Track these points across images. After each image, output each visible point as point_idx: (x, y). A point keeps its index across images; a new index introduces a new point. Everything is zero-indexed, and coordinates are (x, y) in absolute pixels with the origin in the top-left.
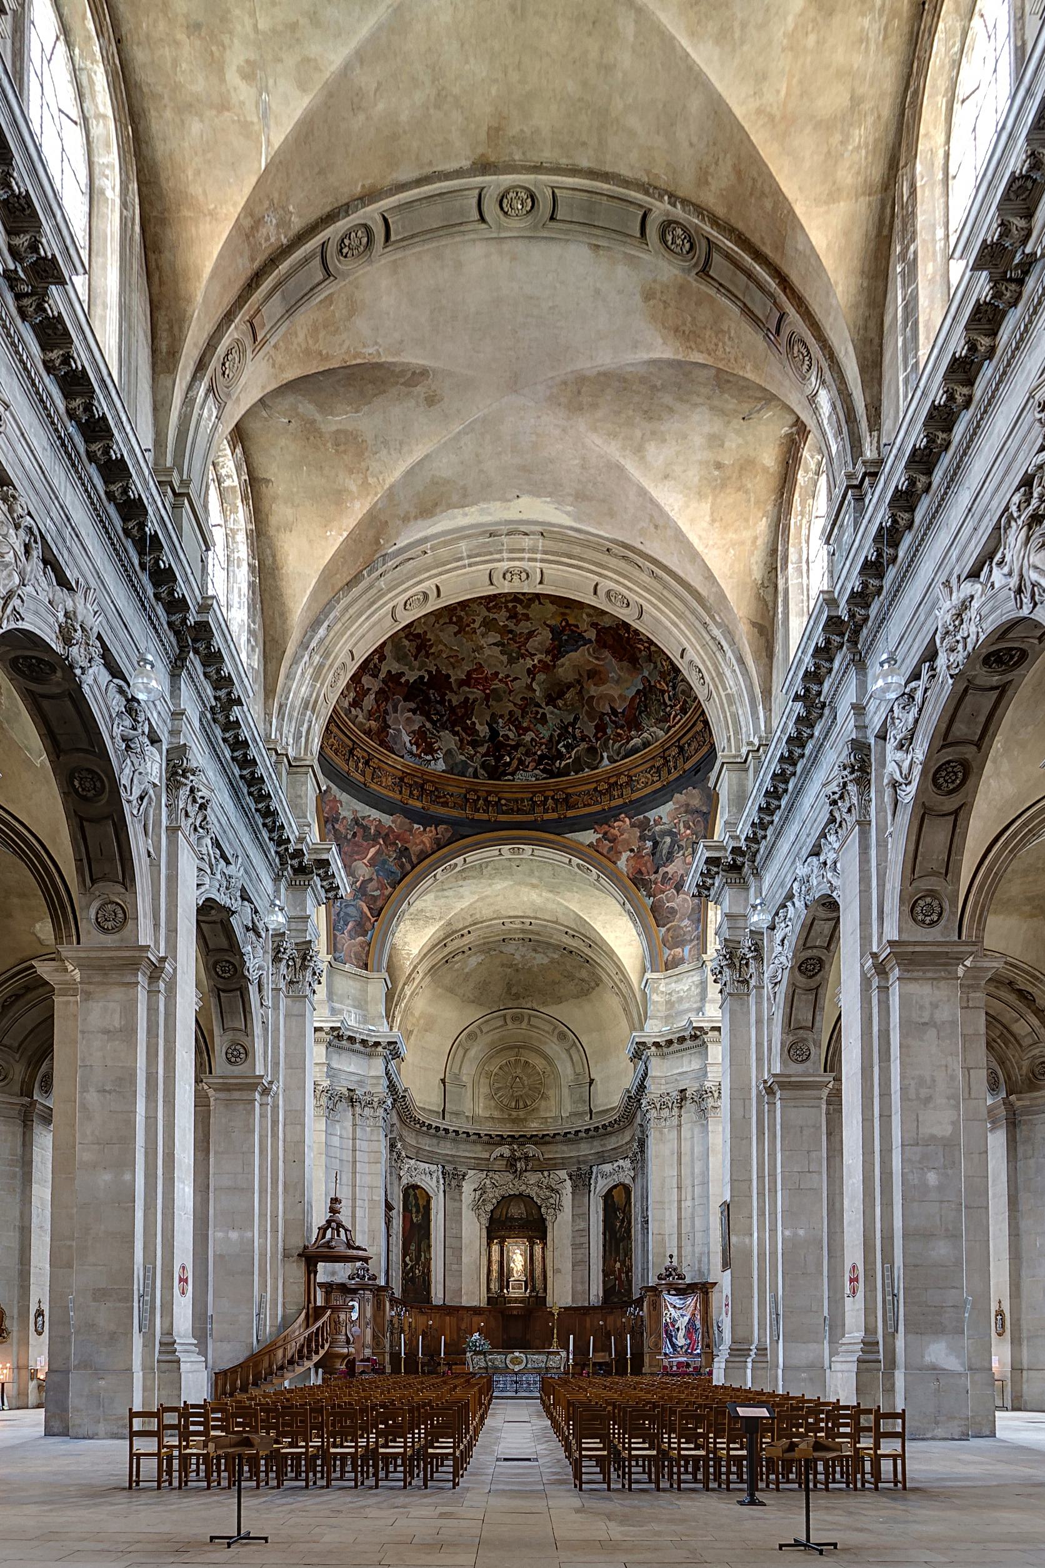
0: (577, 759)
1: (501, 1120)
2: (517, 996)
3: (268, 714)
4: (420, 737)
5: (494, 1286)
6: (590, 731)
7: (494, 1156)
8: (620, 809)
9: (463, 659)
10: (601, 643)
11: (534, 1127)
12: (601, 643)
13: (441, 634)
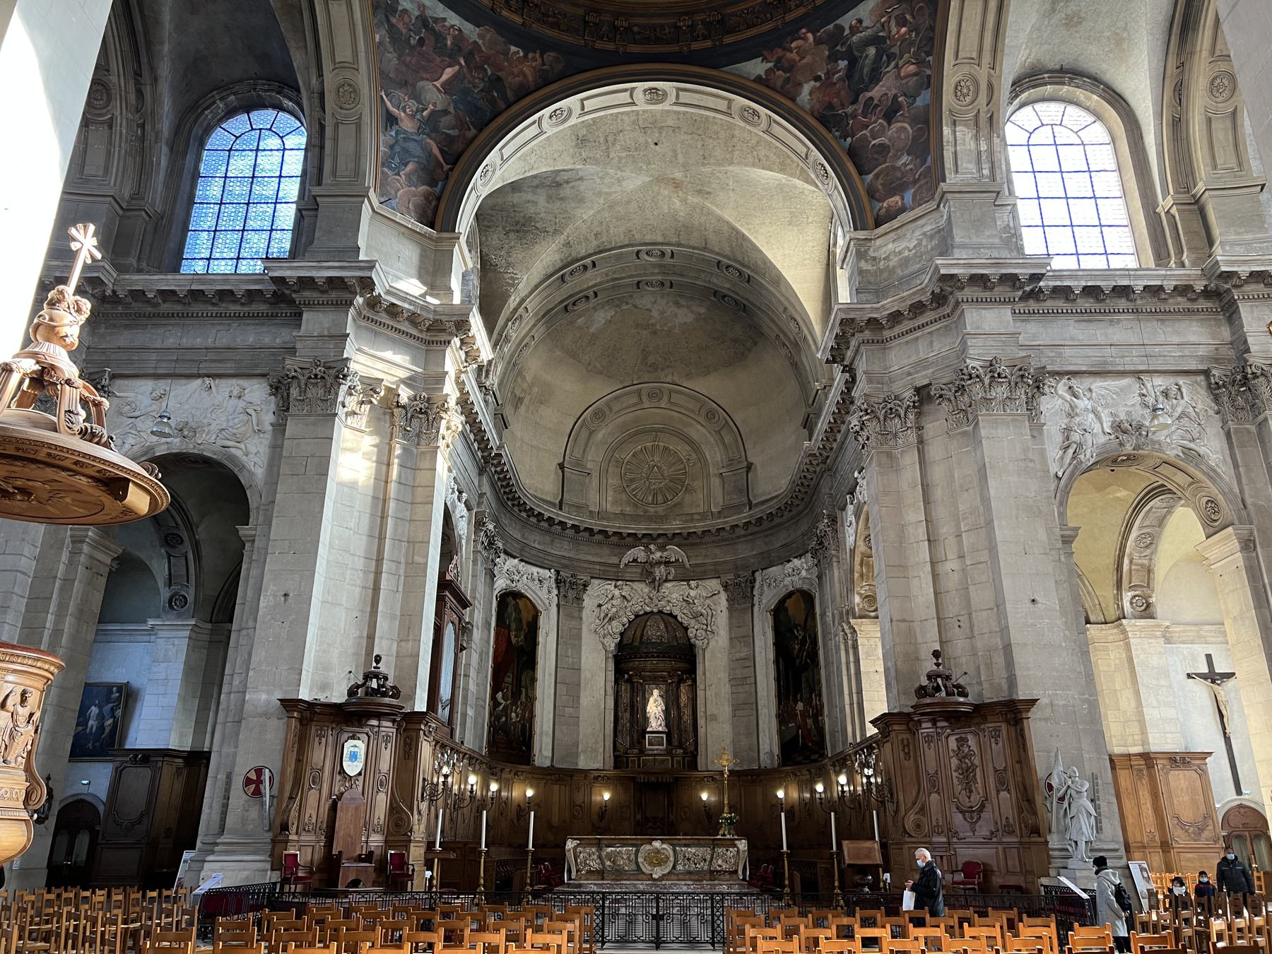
1: (635, 518)
5: (625, 741)
7: (625, 560)
8: (801, 22)
11: (675, 526)
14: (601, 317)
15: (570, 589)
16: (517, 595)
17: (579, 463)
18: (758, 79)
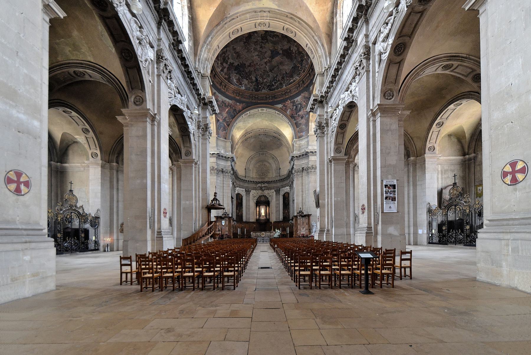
0: (277, 86)
1: (259, 178)
2: (262, 149)
3: (195, 61)
4: (239, 80)
6: (280, 79)
14: (252, 140)
15: (248, 192)
16: (239, 194)
17: (249, 168)
18: (280, 108)
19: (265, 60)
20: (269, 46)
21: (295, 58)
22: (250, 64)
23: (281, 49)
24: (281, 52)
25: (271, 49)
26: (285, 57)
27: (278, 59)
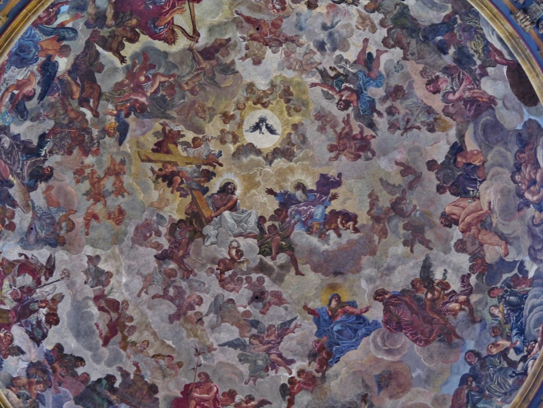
9: (180, 365)
10: (394, 324)
12: (394, 324)
13: (149, 313)
19: (284, 376)
20: (306, 287)
21: (472, 319)
22: (187, 390)
23: (379, 295)
24: (376, 313)
25: (316, 304)
26: (403, 340)
27: (360, 357)
